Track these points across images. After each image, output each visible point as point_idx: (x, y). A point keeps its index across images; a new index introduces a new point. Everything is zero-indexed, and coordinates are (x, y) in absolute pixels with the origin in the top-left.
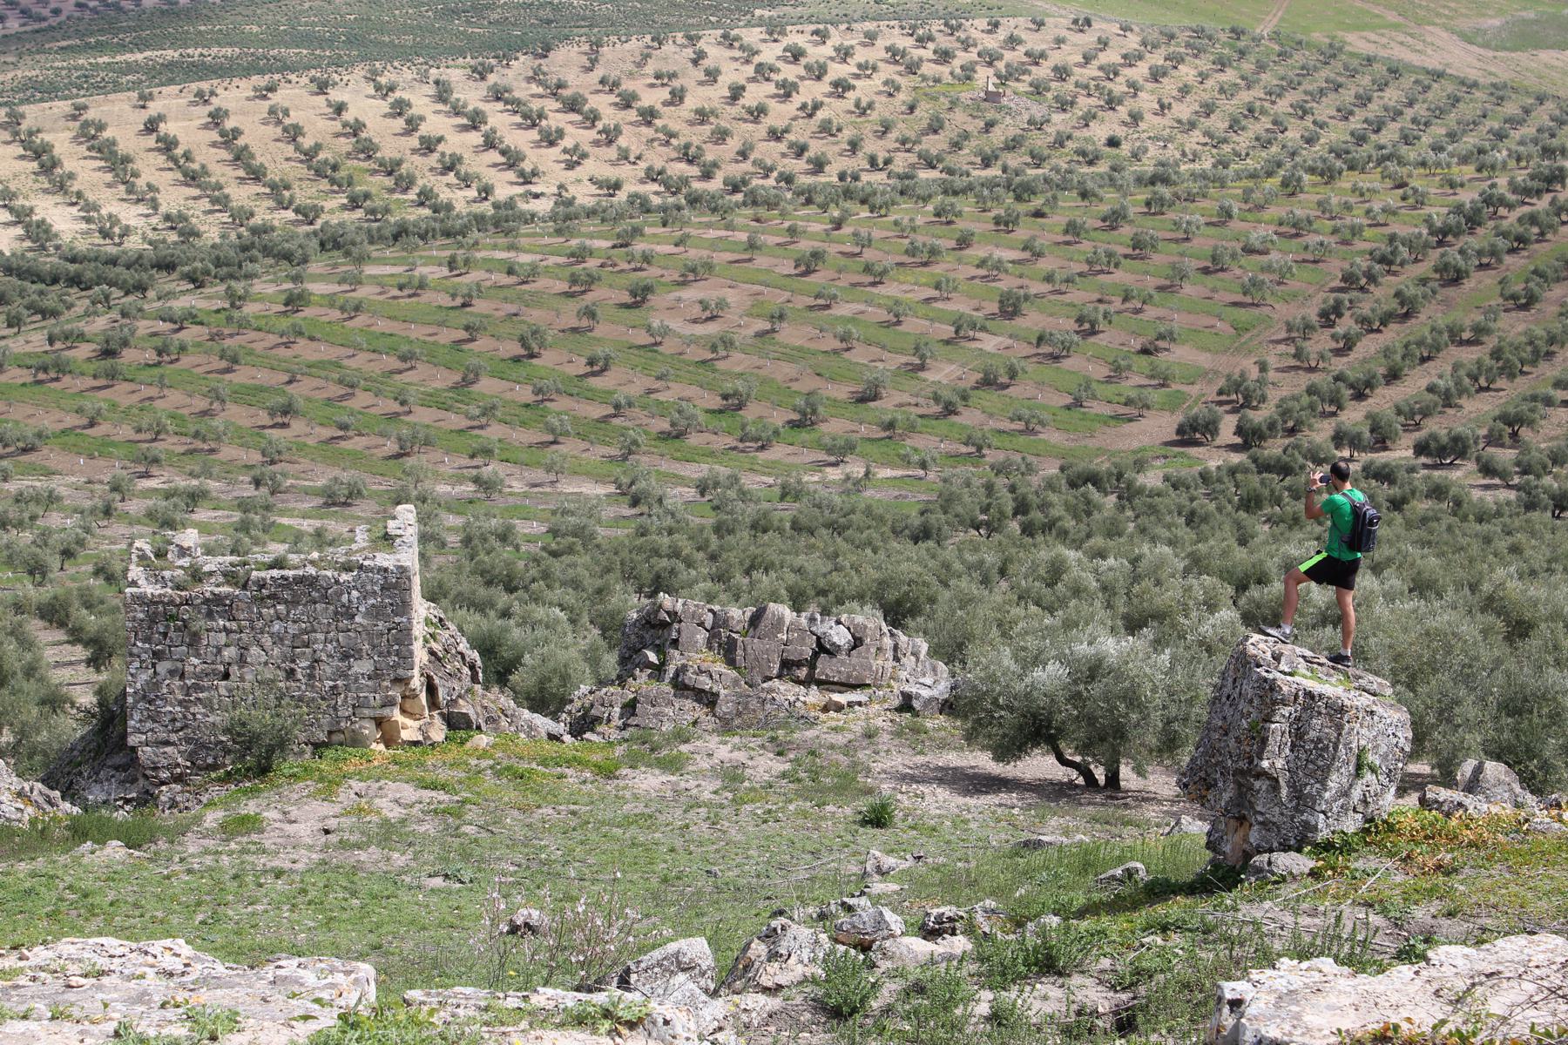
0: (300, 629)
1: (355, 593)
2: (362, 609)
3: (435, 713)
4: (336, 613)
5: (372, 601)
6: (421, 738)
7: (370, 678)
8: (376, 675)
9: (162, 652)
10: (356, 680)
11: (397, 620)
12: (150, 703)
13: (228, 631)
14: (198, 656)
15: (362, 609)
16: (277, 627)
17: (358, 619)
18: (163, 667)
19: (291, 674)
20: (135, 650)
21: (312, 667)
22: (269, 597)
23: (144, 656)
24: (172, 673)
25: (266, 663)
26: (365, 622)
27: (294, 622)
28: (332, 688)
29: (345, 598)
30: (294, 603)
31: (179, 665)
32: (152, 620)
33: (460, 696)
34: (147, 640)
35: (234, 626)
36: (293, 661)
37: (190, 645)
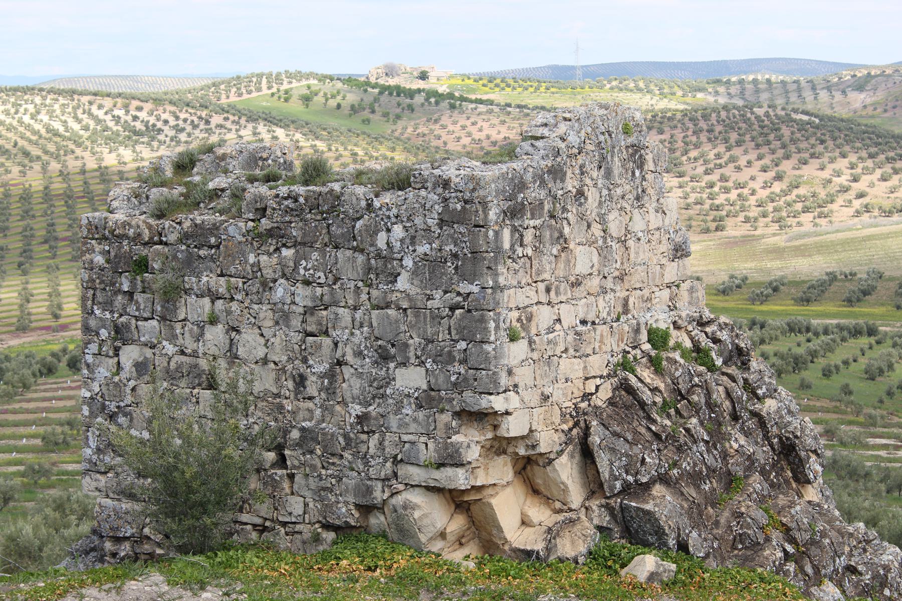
0: (314, 298)
1: (398, 231)
2: (408, 262)
3: (594, 504)
4: (369, 269)
5: (423, 248)
6: (539, 546)
7: (420, 406)
8: (428, 400)
9: (127, 326)
10: (399, 406)
11: (464, 287)
12: (112, 417)
13: (215, 297)
14: (172, 338)
15: (408, 262)
16: (280, 291)
17: (403, 283)
18: (130, 355)
19: (301, 381)
20: (92, 323)
21: (331, 375)
22: (270, 233)
23: (104, 334)
24: (141, 367)
25: (265, 361)
26: (413, 291)
27: (307, 283)
28: (362, 419)
29: (381, 240)
30: (303, 245)
31: (148, 353)
32: (116, 264)
33: (663, 479)
34: (107, 305)
35: (221, 285)
36: (305, 360)
37: (163, 319)
